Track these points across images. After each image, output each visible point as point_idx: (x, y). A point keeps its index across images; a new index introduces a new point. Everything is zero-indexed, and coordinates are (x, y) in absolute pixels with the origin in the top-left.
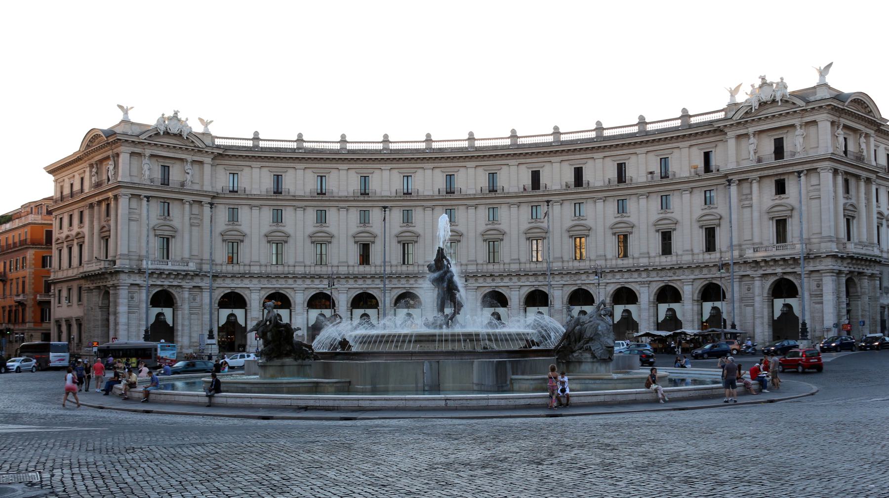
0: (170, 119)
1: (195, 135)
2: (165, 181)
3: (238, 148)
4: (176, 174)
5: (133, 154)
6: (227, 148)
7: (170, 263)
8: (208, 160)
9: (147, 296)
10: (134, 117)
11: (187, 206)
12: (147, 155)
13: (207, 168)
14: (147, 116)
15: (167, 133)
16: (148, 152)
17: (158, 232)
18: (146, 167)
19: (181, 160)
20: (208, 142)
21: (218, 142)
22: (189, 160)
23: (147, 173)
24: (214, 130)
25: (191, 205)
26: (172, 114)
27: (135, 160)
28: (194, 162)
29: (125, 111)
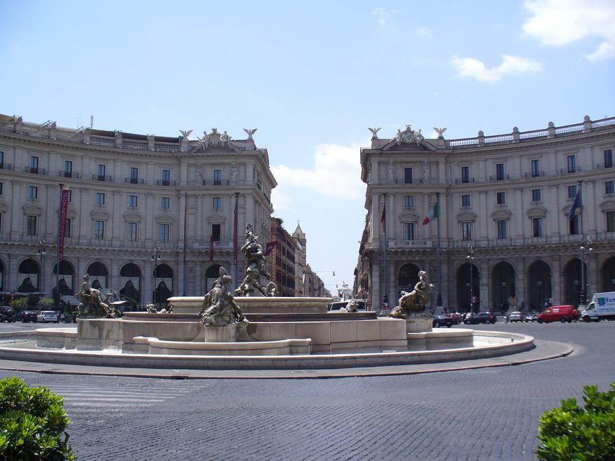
0: (405, 132)
1: (429, 141)
2: (408, 178)
3: (468, 147)
4: (416, 174)
5: (379, 163)
6: (455, 148)
7: (410, 243)
8: (442, 160)
9: (396, 269)
10: (380, 136)
11: (426, 197)
12: (391, 161)
13: (442, 166)
14: (389, 133)
15: (403, 144)
16: (392, 160)
17: (403, 220)
18: (390, 171)
19: (421, 162)
20: (442, 143)
21: (452, 144)
22: (426, 161)
23: (391, 176)
24: (446, 136)
25: (430, 195)
26: (405, 129)
27: (383, 169)
28: (429, 163)
29: (374, 132)
